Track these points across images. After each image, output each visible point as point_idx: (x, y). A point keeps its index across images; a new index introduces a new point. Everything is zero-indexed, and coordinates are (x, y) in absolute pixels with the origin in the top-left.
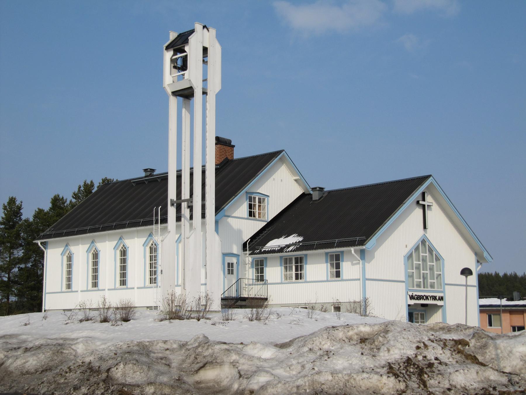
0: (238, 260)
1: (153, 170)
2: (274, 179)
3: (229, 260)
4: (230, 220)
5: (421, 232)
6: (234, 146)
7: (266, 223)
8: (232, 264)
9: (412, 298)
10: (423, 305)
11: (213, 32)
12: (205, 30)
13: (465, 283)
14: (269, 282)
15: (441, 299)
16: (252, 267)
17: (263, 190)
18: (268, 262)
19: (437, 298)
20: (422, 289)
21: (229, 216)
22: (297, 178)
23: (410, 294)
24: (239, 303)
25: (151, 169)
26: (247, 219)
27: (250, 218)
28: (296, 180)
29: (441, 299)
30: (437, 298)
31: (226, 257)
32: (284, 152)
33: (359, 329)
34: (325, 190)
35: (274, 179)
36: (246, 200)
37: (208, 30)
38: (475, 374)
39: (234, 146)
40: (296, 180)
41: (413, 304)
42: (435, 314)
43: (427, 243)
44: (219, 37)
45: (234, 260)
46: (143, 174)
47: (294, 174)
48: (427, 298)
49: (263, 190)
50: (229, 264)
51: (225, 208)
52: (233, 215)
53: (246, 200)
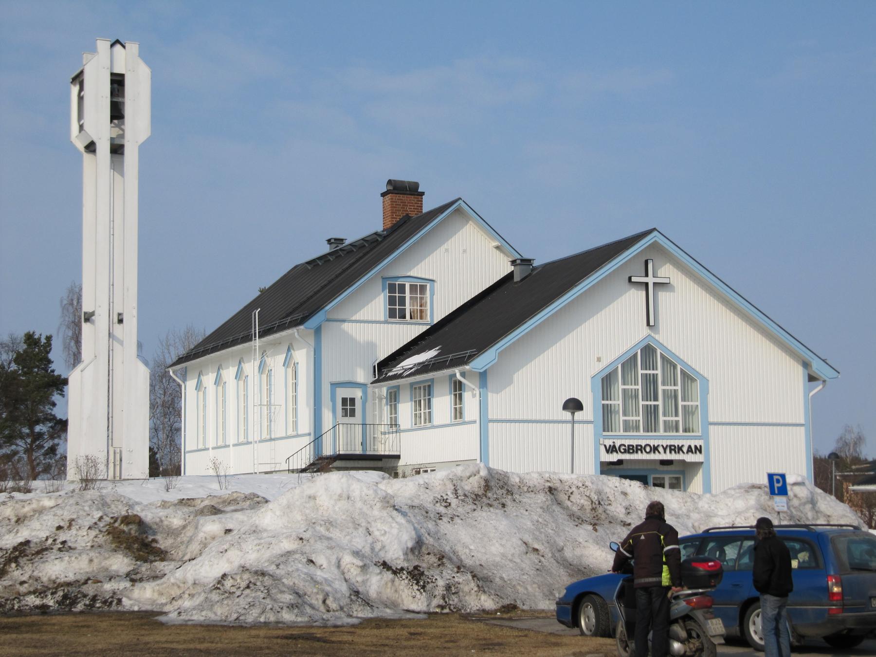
0: (365, 393)
1: (340, 241)
2: (447, 250)
3: (347, 393)
4: (346, 326)
5: (645, 331)
6: (423, 194)
7: (428, 327)
8: (353, 401)
9: (611, 449)
10: (664, 462)
11: (133, 48)
12: (118, 47)
13: (569, 426)
14: (402, 428)
15: (698, 450)
16: (387, 404)
17: (421, 269)
18: (401, 392)
19: (685, 449)
20: (641, 433)
21: (344, 321)
22: (496, 244)
23: (609, 443)
24: (338, 464)
25: (335, 239)
26: (386, 322)
27: (393, 320)
28: (497, 248)
29: (698, 450)
30: (685, 449)
31: (338, 389)
32: (460, 202)
33: (41, 503)
34: (536, 264)
35: (447, 250)
36: (383, 290)
37: (124, 47)
38: (86, 562)
39: (423, 194)
40: (497, 248)
41: (615, 460)
42: (695, 478)
43: (659, 351)
44: (146, 55)
45: (358, 394)
46: (326, 249)
47: (494, 239)
48: (655, 449)
49: (421, 269)
50: (344, 401)
51: (327, 308)
52: (354, 318)
53: (383, 290)
